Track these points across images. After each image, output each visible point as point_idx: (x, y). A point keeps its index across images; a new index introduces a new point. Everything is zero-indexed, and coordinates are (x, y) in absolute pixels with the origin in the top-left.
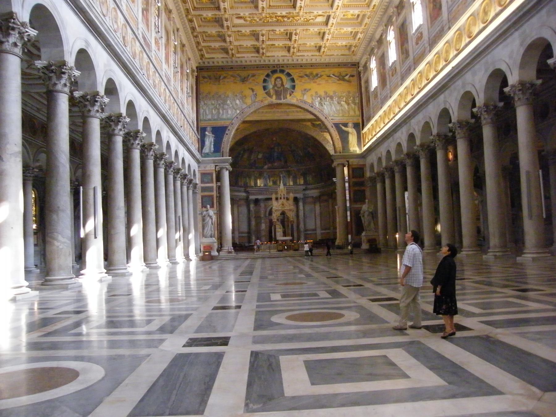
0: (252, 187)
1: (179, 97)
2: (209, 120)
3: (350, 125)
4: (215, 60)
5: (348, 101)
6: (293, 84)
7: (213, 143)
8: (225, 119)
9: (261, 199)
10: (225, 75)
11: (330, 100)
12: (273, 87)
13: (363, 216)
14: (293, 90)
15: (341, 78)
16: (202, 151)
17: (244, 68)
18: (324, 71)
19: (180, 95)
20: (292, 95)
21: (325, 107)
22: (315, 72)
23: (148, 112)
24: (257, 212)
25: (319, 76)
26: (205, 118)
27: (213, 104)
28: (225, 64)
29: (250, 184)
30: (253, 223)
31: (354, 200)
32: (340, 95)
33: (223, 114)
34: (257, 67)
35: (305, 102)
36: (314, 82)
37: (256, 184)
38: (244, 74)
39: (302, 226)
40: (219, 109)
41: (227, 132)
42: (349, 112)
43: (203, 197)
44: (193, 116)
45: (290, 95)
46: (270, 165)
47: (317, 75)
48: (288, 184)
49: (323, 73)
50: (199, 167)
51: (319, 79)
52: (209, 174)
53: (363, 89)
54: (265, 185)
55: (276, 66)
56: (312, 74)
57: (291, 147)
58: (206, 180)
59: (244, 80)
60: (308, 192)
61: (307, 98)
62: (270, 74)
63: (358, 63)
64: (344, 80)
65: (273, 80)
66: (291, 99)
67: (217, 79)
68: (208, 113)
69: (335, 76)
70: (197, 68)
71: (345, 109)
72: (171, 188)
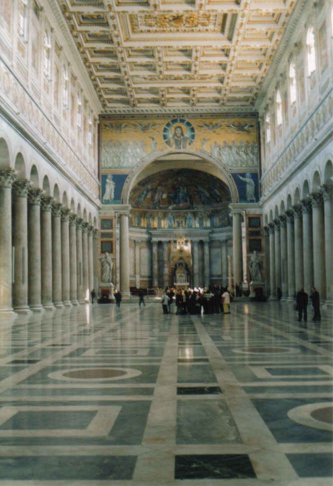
0: (155, 229)
1: (83, 153)
2: (110, 168)
3: (248, 175)
4: (117, 109)
5: (247, 151)
6: (193, 133)
7: (113, 191)
8: (125, 168)
9: (165, 242)
10: (126, 124)
11: (229, 151)
12: (174, 136)
13: (251, 266)
14: (192, 140)
15: (240, 128)
16: (102, 197)
17: (145, 117)
18: (224, 122)
19: (83, 151)
20: (192, 145)
21: (224, 157)
22: (214, 122)
23: (57, 179)
24: (160, 255)
25: (218, 126)
26: (106, 166)
27: (113, 152)
28: (127, 113)
29: (154, 225)
30: (156, 267)
31: (250, 250)
32: (239, 144)
33: (124, 163)
34: (158, 116)
35: (204, 152)
36: (215, 132)
37: (159, 224)
38: (145, 122)
39: (207, 271)
40: (120, 157)
41: (127, 180)
42: (247, 162)
43: (102, 242)
44: (95, 165)
45: (190, 144)
46: (175, 205)
47: (217, 124)
48: (193, 226)
49: (223, 124)
50: (99, 213)
51: (219, 129)
52: (108, 220)
53: (262, 140)
54: (170, 227)
55: (176, 115)
56: (211, 123)
57: (197, 188)
58: (106, 226)
59: (145, 128)
60: (215, 235)
61: (206, 147)
62: (171, 123)
63: (258, 113)
64: (245, 130)
65: (173, 129)
66: (189, 149)
67: (119, 127)
68: (109, 161)
69: (235, 126)
70: (99, 116)
71: (244, 159)
72: (74, 237)
